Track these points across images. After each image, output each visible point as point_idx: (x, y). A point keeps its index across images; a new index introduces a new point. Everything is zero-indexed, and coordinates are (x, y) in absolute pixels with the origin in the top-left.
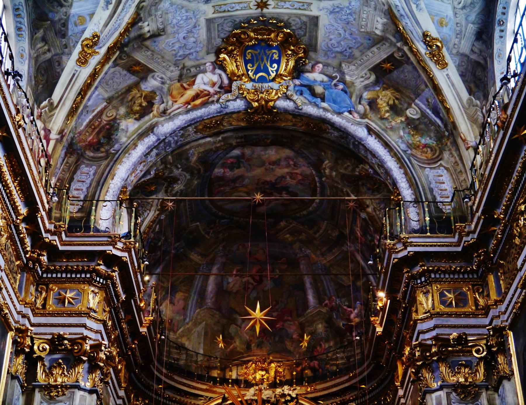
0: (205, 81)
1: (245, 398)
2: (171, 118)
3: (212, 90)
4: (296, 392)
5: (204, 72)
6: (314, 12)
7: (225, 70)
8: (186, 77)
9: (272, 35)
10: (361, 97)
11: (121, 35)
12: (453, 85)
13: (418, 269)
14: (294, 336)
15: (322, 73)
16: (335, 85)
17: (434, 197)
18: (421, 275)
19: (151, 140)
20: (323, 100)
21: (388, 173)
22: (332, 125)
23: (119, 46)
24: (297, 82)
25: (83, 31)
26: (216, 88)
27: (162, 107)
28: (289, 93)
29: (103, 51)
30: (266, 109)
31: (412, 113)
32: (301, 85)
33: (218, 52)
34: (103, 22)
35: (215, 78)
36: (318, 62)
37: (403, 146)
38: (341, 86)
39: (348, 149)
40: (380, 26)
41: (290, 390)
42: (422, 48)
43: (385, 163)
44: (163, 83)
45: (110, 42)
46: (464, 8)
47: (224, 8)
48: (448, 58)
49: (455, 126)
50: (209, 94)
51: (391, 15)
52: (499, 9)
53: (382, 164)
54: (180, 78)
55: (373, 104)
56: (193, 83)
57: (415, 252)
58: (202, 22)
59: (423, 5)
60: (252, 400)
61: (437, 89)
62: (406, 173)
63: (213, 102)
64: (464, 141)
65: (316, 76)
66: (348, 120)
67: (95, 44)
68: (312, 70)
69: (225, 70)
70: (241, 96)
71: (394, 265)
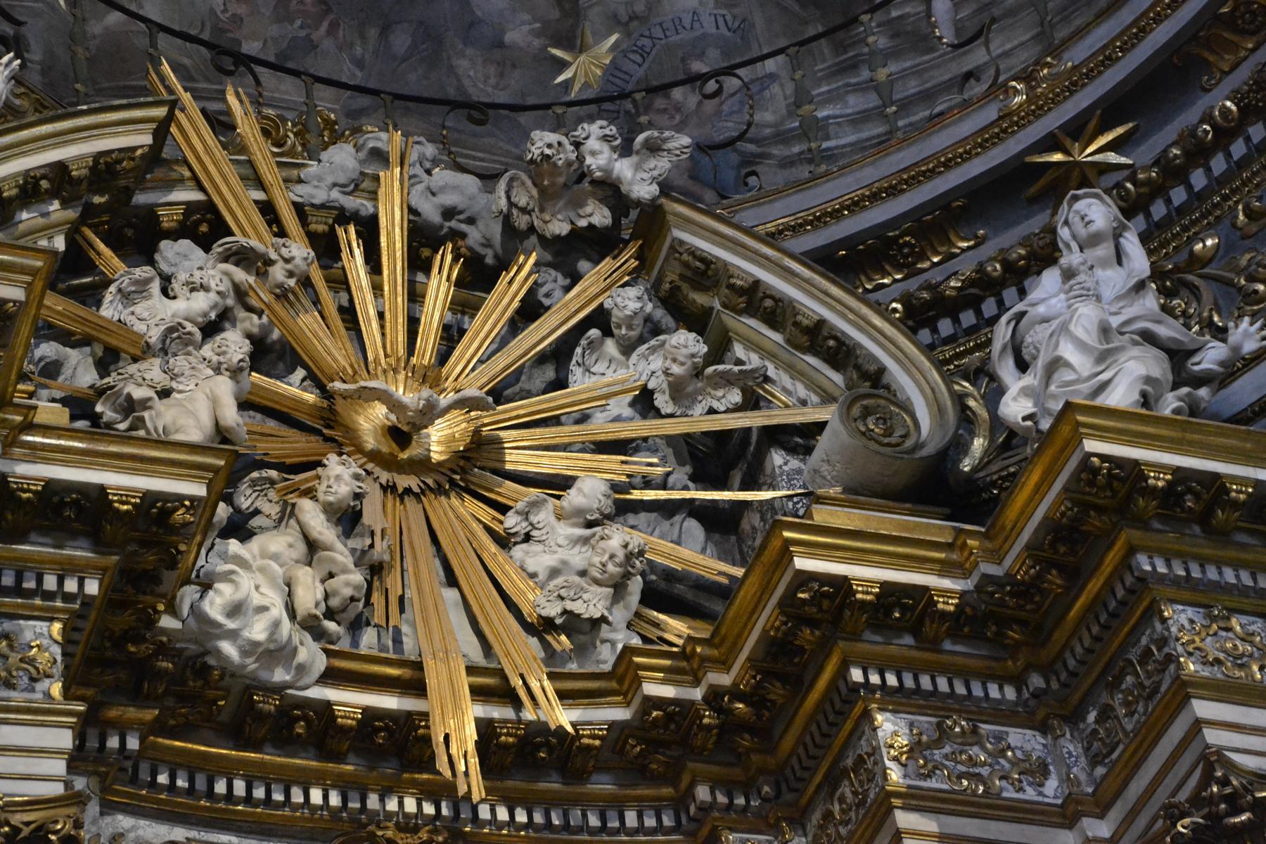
1: (302, 192)
4: (661, 164)
14: (513, 36)
41: (625, 150)
60: (344, 217)
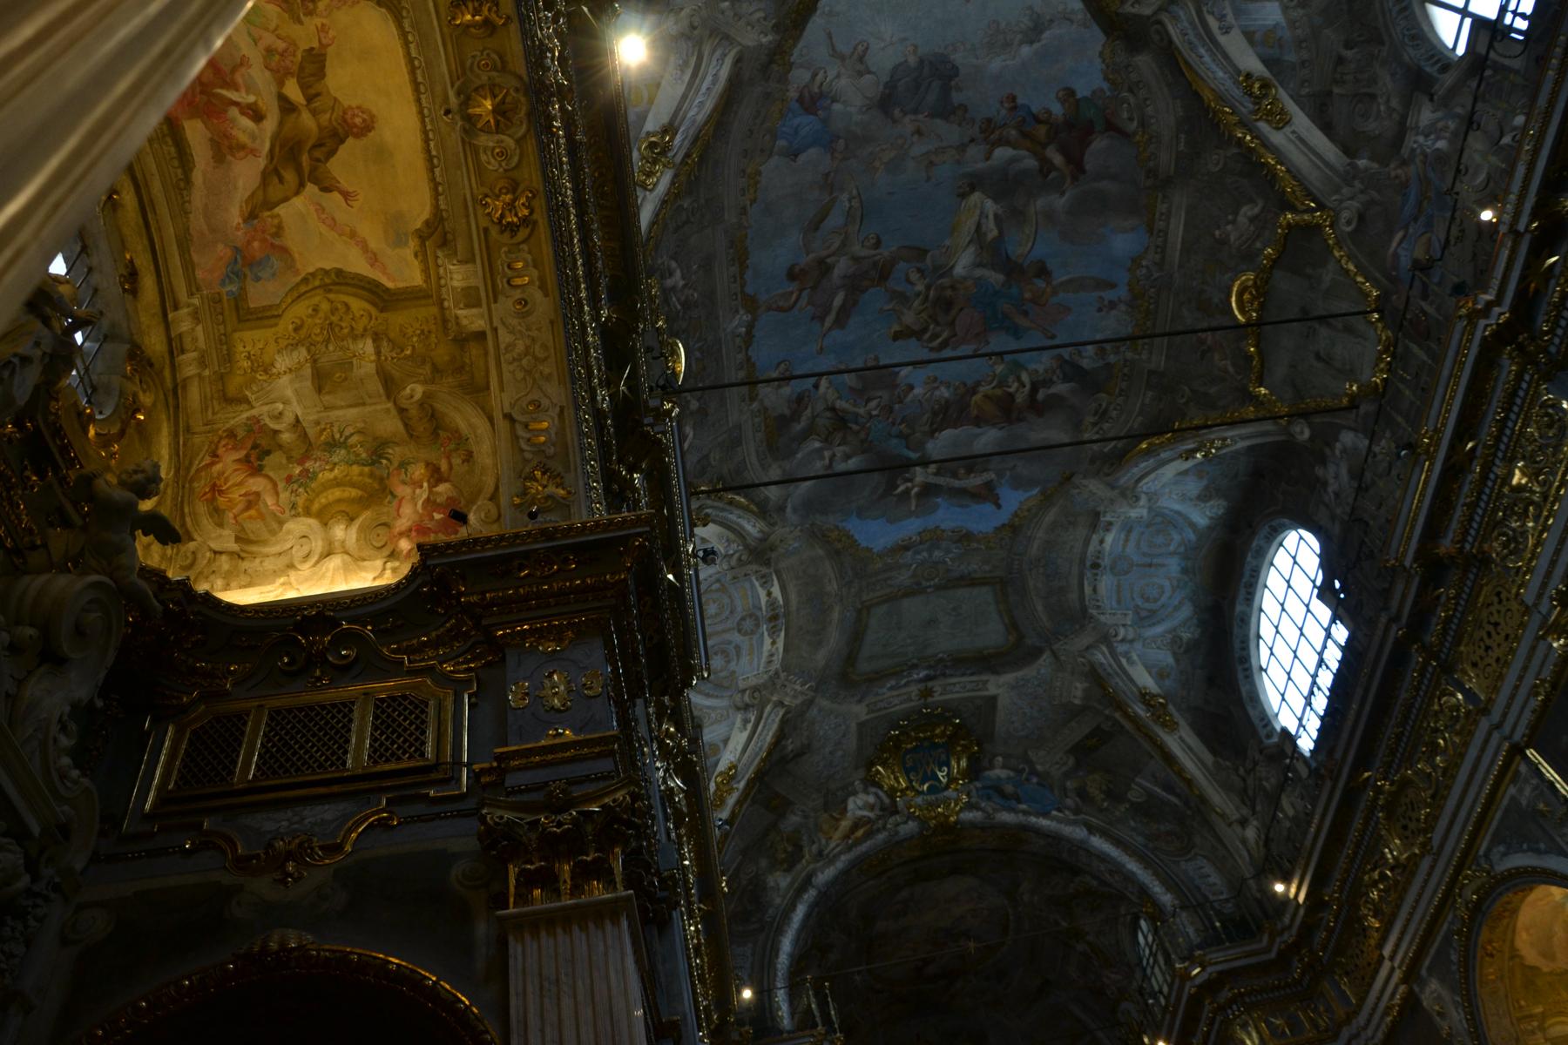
0: (858, 805)
2: (832, 861)
3: (871, 815)
5: (855, 793)
6: (992, 690)
7: (881, 787)
8: (835, 803)
9: (938, 731)
10: (1065, 789)
11: (763, 760)
12: (1190, 748)
13: (1225, 994)
15: (1004, 767)
16: (1027, 780)
17: (1204, 896)
18: (1231, 1002)
19: (810, 895)
20: (1019, 801)
21: (1129, 878)
22: (1038, 831)
23: (760, 777)
24: (978, 785)
25: (716, 764)
26: (878, 812)
27: (815, 848)
28: (974, 800)
29: (742, 785)
30: (948, 829)
31: (1134, 795)
32: (984, 788)
33: (873, 764)
34: (740, 748)
35: (871, 799)
36: (995, 756)
37: (1140, 839)
38: (1035, 780)
39: (1061, 861)
40: (1079, 693)
42: (1141, 711)
43: (1124, 866)
44: (806, 817)
45: (750, 773)
46: (1186, 652)
47: (882, 705)
48: (1177, 716)
49: (1203, 800)
50: (869, 821)
51: (1096, 677)
52: (1237, 645)
53: (1118, 869)
54: (826, 807)
55: (1082, 793)
56: (845, 810)
57: (1220, 973)
58: (853, 726)
59: (1135, 658)
61: (1169, 758)
62: (1156, 874)
63: (878, 831)
64: (1223, 816)
65: (999, 772)
66: (1059, 821)
67: (732, 778)
68: (992, 767)
69: (881, 787)
70: (911, 817)
71: (1191, 996)
